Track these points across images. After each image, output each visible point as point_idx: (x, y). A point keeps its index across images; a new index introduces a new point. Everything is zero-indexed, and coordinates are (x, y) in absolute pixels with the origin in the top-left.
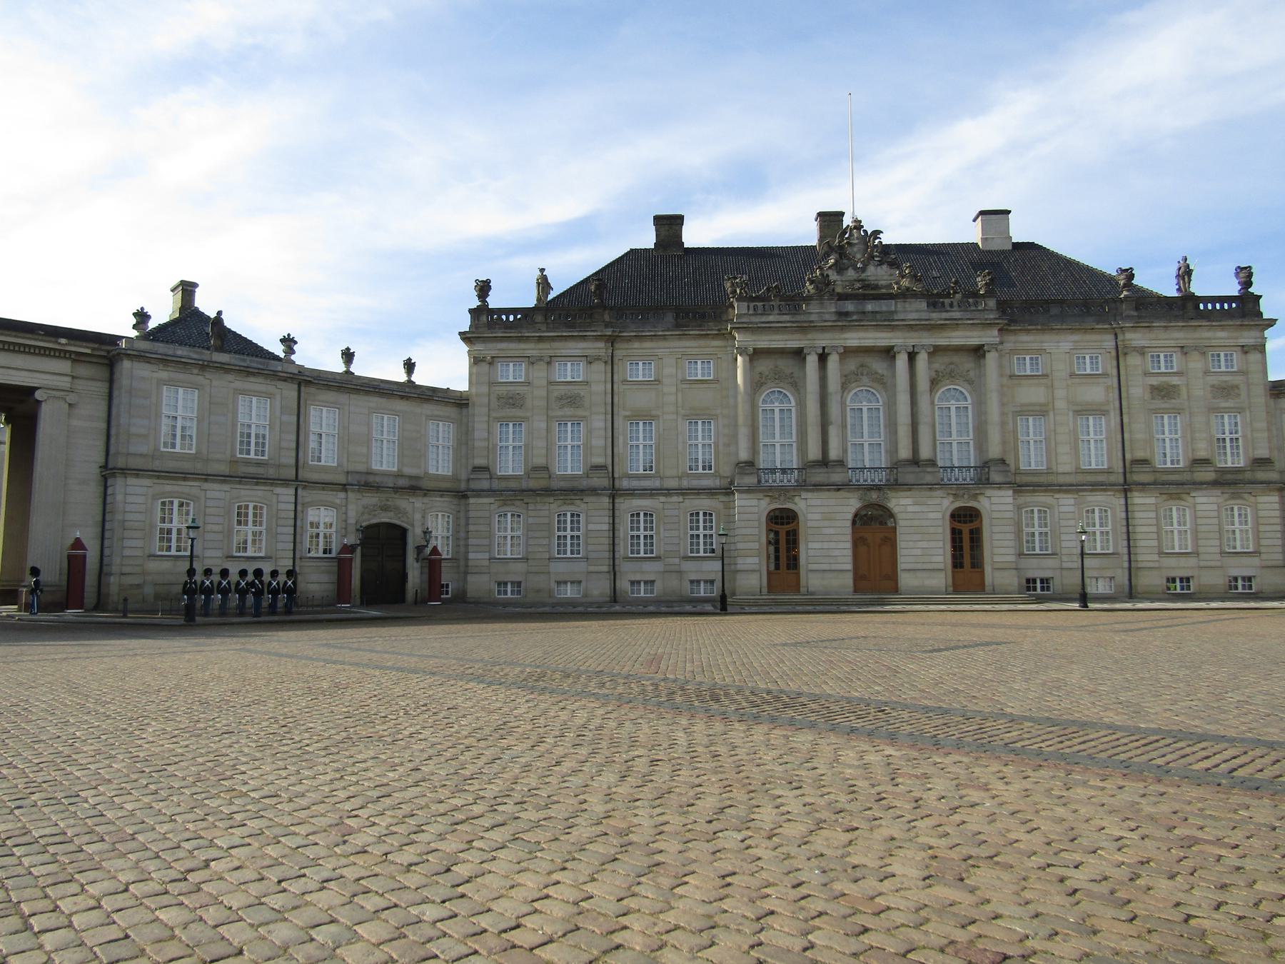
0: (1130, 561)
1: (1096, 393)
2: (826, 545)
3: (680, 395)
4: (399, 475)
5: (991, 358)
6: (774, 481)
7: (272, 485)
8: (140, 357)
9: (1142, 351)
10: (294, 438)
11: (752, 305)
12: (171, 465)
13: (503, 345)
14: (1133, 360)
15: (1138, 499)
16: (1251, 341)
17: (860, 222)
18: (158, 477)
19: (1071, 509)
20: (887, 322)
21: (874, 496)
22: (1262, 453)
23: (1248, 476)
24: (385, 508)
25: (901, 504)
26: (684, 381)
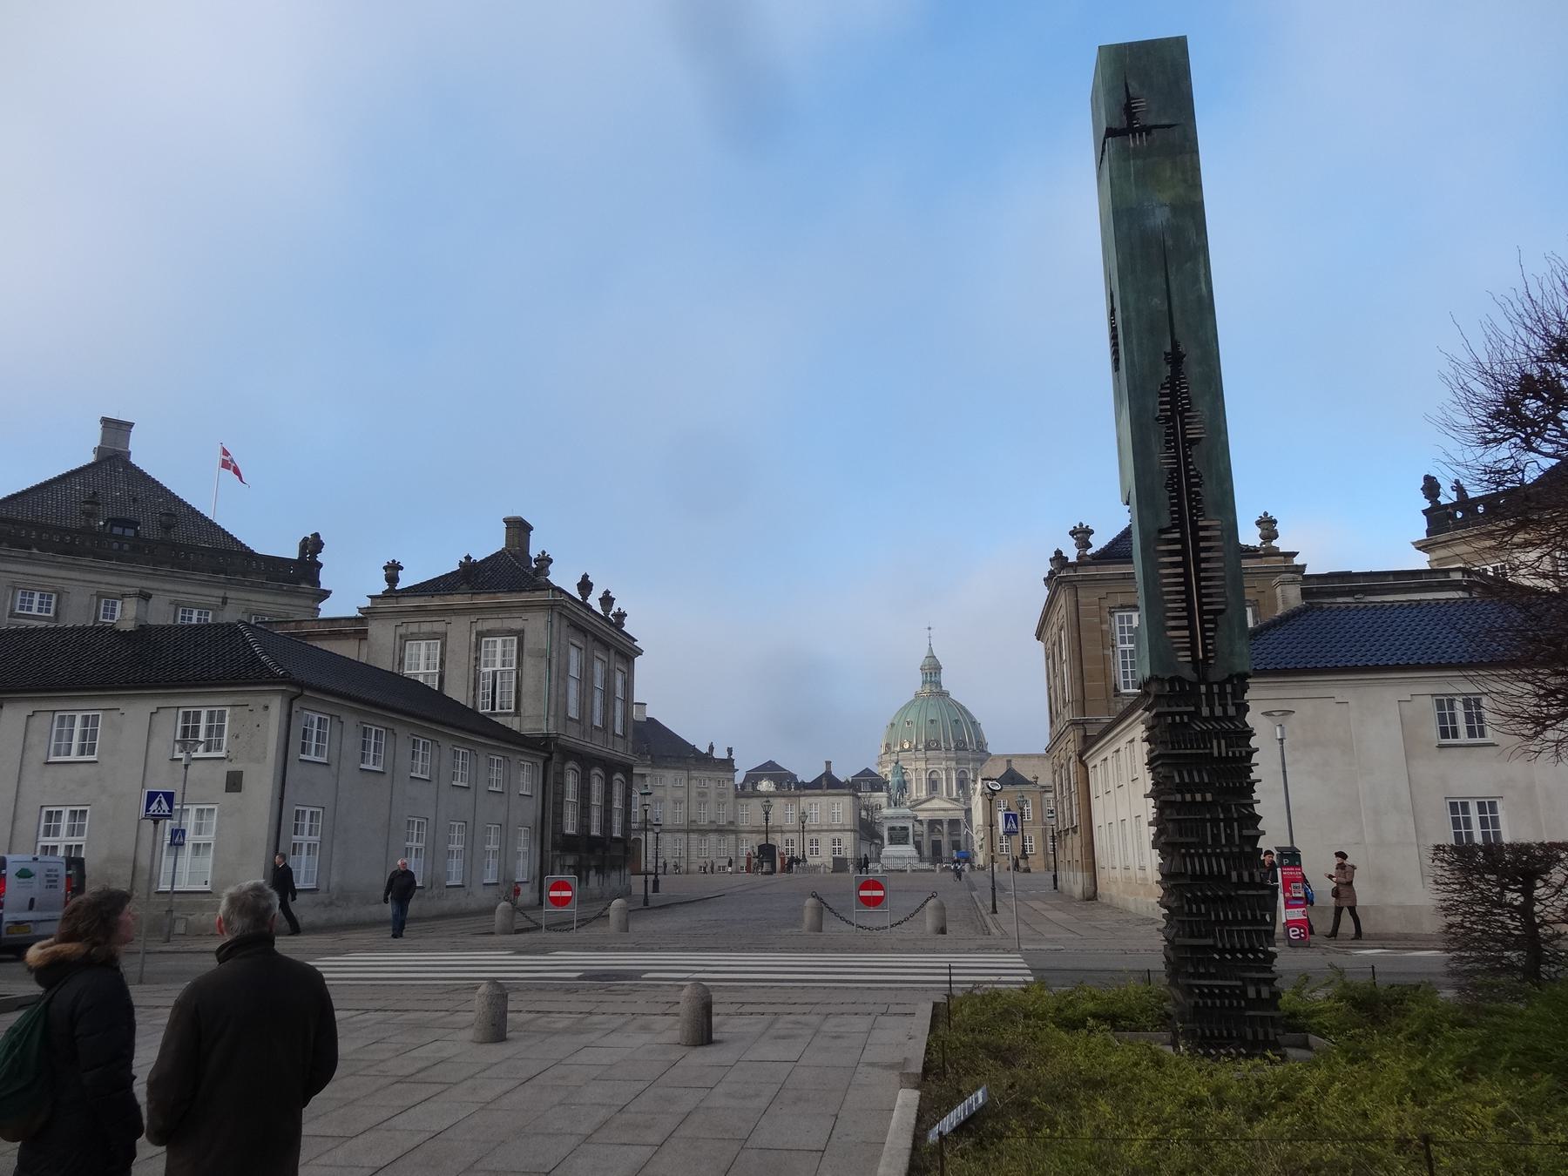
1: (680, 794)
5: (648, 779)
9: (696, 779)
14: (694, 783)
15: (693, 836)
22: (732, 820)
23: (726, 828)
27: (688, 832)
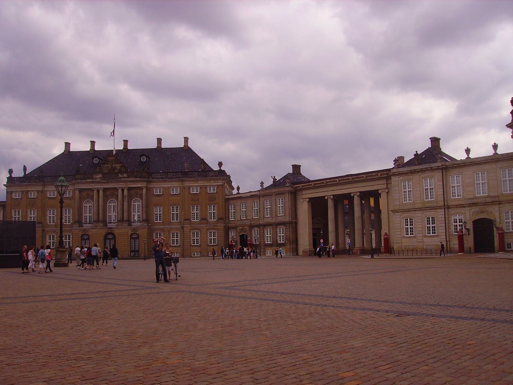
4: (489, 197)
7: (435, 209)
8: (394, 175)
10: (442, 190)
12: (406, 207)
18: (402, 211)
24: (482, 212)
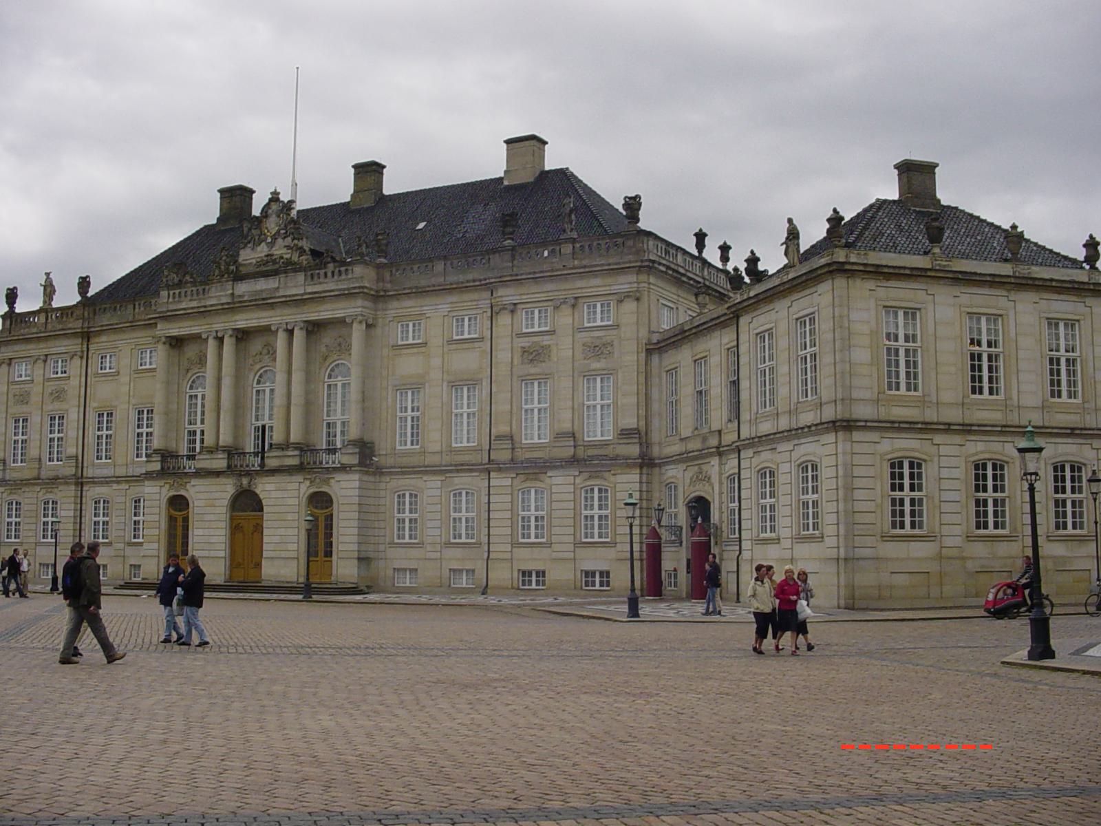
0: (489, 551)
1: (469, 361)
2: (206, 532)
3: (132, 384)
5: (357, 332)
6: (241, 466)
11: (171, 292)
13: (16, 348)
14: (504, 320)
16: (625, 288)
17: (279, 193)
19: (438, 492)
20: (263, 303)
21: (245, 481)
25: (266, 488)
26: (137, 371)
27: (489, 468)
